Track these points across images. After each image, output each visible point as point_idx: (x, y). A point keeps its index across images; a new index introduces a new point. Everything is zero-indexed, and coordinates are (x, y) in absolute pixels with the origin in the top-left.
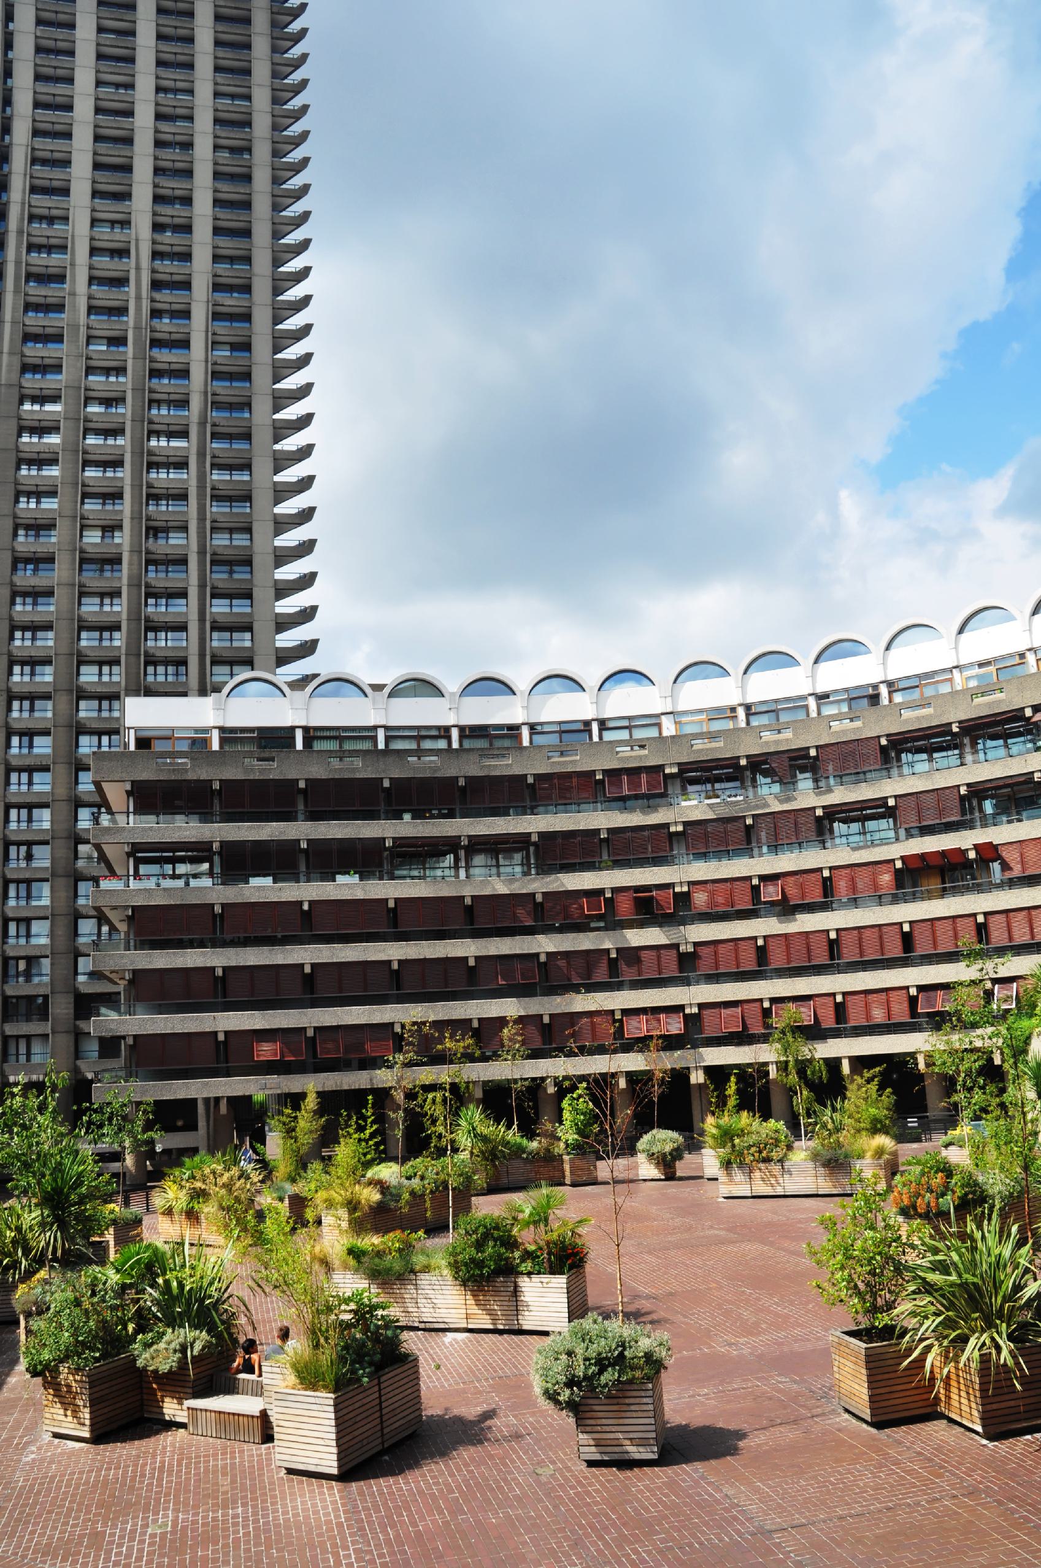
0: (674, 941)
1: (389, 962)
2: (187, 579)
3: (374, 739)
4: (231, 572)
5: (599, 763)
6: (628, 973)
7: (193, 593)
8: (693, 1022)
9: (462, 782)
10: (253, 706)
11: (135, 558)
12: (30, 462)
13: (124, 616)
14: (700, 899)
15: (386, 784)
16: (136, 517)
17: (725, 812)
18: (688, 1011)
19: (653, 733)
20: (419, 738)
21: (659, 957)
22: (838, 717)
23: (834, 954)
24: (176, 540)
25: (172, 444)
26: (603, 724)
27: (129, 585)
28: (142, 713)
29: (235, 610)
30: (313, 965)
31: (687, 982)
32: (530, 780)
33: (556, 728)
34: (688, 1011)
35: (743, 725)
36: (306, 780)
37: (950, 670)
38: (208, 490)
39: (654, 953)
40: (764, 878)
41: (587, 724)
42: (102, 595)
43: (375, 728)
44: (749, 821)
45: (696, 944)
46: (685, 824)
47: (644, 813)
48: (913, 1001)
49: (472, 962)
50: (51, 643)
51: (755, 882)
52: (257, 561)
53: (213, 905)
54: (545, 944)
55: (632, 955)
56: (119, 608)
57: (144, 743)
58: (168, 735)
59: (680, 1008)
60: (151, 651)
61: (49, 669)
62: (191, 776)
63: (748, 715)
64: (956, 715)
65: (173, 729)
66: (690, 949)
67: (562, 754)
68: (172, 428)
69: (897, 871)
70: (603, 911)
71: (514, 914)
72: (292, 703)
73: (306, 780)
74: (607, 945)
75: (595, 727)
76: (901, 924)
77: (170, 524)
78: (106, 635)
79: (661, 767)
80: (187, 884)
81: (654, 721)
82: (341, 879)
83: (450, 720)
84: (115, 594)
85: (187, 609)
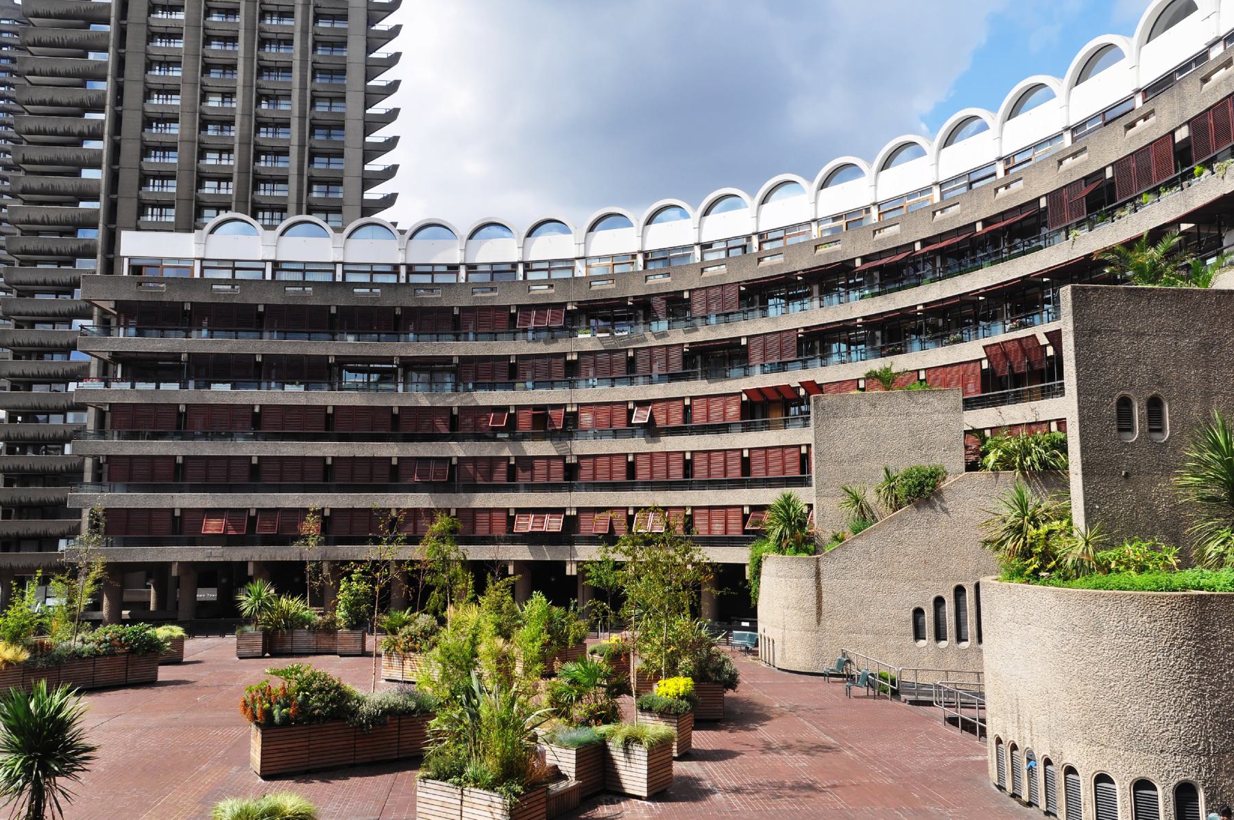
0: (563, 453)
1: (324, 458)
2: (289, 140)
3: (334, 272)
4: (329, 135)
5: (512, 299)
6: (523, 477)
7: (294, 151)
8: (571, 524)
9: (398, 312)
10: (312, 246)
11: (246, 120)
12: (162, 36)
13: (236, 169)
14: (586, 419)
15: (333, 310)
16: (247, 85)
17: (611, 344)
18: (568, 513)
19: (568, 274)
20: (372, 273)
21: (549, 466)
22: (718, 263)
23: (689, 474)
24: (283, 106)
25: (336, 25)
26: (528, 266)
27: (240, 143)
28: (133, 244)
29: (332, 167)
30: (259, 458)
31: (571, 488)
32: (456, 312)
33: (488, 268)
34: (568, 513)
35: (641, 269)
36: (265, 305)
37: (809, 223)
38: (310, 63)
39: (544, 462)
40: (641, 404)
41: (514, 265)
42: (328, 155)
43: (335, 263)
44: (631, 354)
45: (580, 457)
46: (579, 354)
47: (546, 342)
48: (745, 518)
49: (394, 462)
50: (174, 190)
51: (631, 406)
52: (348, 125)
53: (178, 405)
54: (457, 450)
55: (527, 462)
56: (290, 164)
57: (136, 269)
58: (157, 264)
59: (561, 510)
60: (257, 199)
61: (172, 212)
62: (165, 299)
63: (645, 262)
64: (802, 263)
65: (161, 259)
66: (574, 461)
67: (492, 290)
68: (281, 9)
69: (743, 402)
70: (508, 424)
71: (433, 423)
72: (263, 240)
73: (265, 305)
74: (506, 452)
75: (521, 268)
76: (742, 450)
77: (277, 92)
78: (223, 184)
79: (565, 304)
80: (158, 387)
81: (569, 263)
82: (288, 388)
83: (399, 259)
84: (230, 151)
85: (290, 164)
